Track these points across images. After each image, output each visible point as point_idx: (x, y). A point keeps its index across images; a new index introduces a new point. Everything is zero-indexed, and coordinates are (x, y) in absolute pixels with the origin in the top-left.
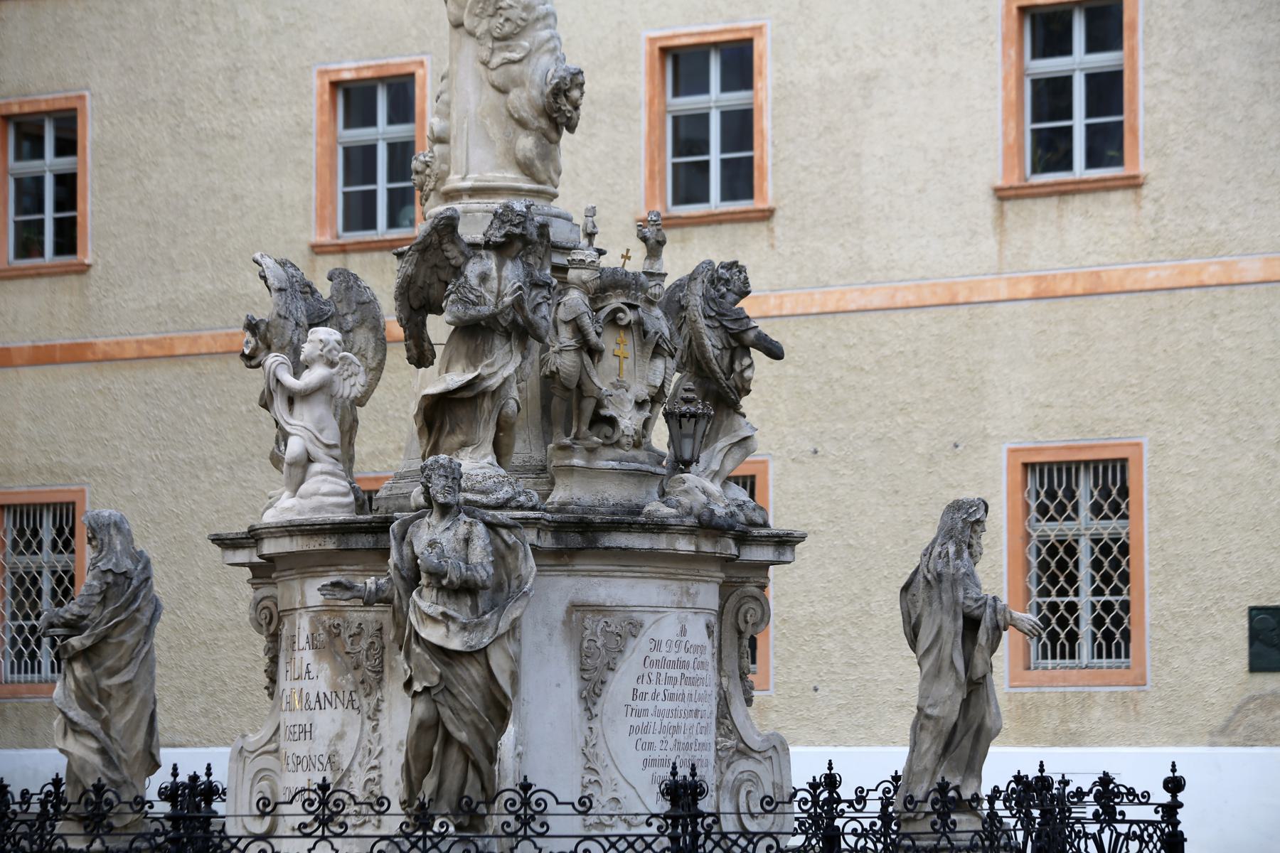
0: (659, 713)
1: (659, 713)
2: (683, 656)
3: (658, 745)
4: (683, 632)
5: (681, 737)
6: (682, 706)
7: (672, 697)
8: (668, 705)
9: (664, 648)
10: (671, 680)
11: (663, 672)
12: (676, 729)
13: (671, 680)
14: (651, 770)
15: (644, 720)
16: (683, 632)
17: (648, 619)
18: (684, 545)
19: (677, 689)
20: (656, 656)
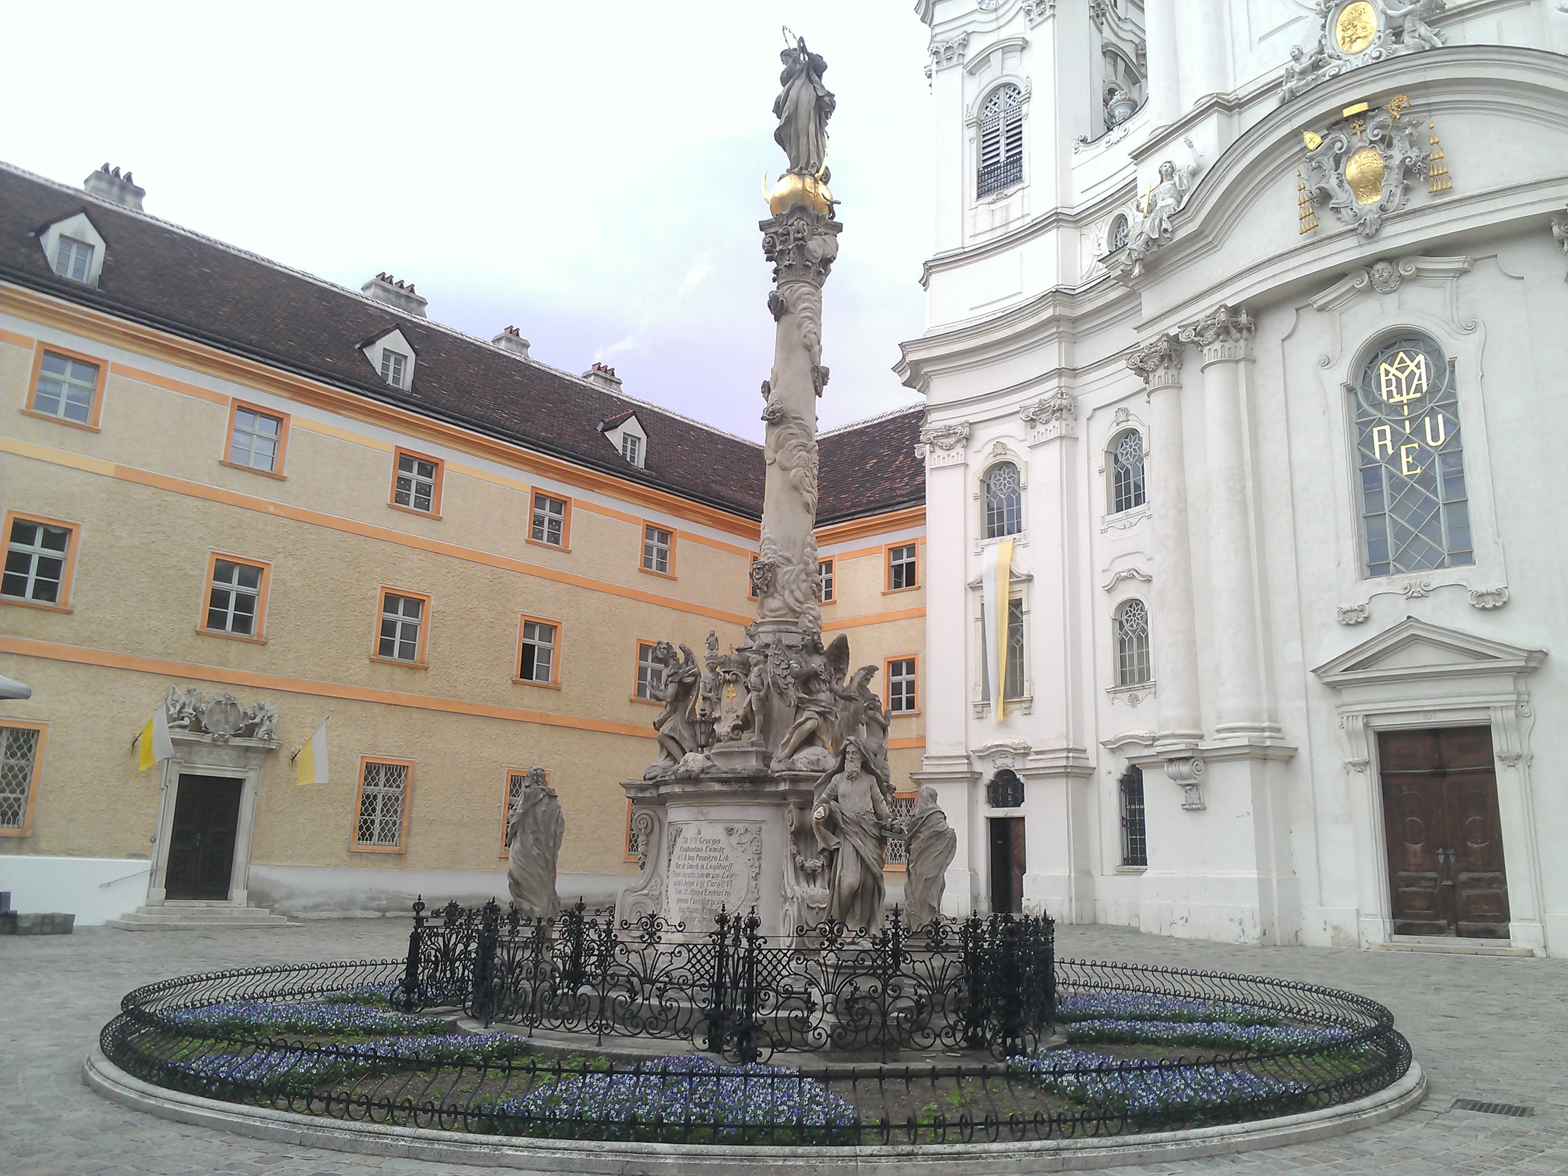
0: (684, 875)
1: (684, 875)
2: (698, 845)
3: (683, 891)
4: (699, 833)
5: (694, 887)
6: (696, 871)
7: (691, 867)
8: (690, 871)
9: (689, 841)
10: (690, 858)
11: (687, 854)
12: (692, 883)
13: (690, 858)
14: (680, 904)
15: (679, 878)
16: (699, 833)
17: (684, 827)
18: (677, 789)
19: (694, 863)
20: (685, 846)
